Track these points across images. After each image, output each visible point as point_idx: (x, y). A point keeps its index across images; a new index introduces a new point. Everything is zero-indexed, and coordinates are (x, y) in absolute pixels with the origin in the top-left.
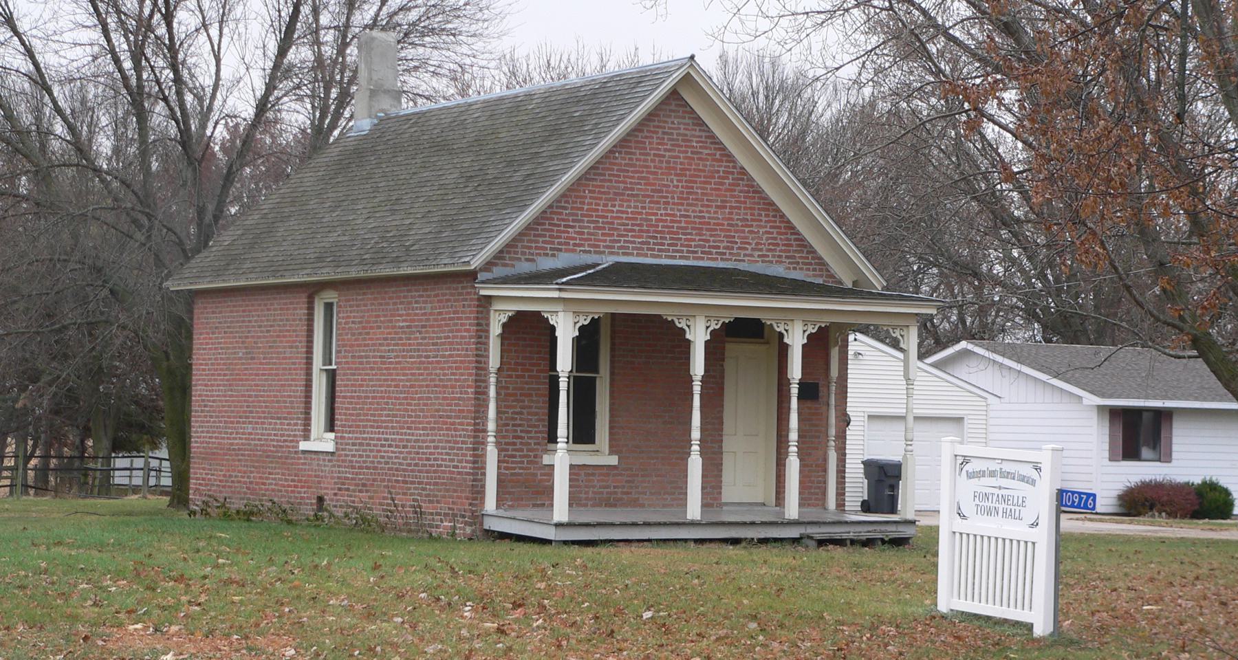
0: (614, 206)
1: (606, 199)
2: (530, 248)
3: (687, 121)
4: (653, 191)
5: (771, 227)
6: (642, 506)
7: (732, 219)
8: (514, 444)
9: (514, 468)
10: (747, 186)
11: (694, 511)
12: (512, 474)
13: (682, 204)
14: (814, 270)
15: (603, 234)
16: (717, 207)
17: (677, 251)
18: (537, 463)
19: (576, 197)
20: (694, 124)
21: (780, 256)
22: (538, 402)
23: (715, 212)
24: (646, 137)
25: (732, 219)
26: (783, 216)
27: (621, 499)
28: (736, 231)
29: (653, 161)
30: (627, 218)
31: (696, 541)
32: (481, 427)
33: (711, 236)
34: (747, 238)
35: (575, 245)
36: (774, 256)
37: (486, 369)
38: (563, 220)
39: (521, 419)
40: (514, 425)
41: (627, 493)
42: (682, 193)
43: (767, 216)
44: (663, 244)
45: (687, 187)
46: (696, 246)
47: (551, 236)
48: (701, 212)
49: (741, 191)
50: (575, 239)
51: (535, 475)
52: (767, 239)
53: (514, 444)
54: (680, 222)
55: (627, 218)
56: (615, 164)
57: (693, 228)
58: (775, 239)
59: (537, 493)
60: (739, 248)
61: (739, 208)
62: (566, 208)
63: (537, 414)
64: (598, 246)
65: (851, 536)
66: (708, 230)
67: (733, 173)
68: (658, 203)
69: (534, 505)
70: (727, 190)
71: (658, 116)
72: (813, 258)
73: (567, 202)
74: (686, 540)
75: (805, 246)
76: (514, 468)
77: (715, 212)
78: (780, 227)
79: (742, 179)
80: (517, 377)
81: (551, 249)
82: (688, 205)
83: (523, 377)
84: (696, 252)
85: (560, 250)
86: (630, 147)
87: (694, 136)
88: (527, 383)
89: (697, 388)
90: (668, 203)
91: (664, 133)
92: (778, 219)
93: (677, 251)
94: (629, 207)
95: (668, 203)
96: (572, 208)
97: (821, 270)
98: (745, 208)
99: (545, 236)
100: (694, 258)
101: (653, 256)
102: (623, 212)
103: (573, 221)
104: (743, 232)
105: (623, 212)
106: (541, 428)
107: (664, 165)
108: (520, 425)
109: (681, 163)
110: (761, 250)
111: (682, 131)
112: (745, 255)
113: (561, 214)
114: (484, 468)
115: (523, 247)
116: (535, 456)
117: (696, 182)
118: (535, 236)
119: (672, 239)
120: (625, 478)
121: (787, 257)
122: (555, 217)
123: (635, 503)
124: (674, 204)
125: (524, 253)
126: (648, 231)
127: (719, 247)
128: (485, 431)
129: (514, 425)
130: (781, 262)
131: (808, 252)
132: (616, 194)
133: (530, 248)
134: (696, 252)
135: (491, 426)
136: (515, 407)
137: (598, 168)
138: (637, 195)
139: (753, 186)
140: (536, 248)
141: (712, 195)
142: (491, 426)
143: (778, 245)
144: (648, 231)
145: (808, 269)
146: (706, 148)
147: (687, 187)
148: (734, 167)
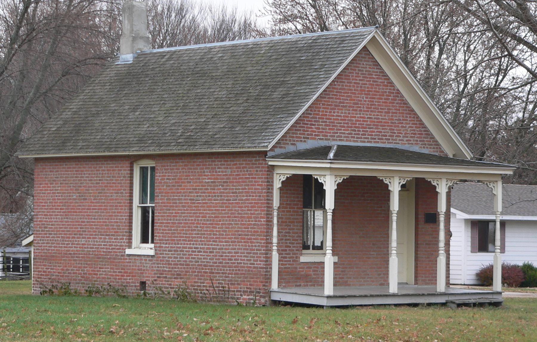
0: (334, 112)
1: (331, 109)
2: (293, 137)
3: (370, 63)
4: (354, 104)
5: (413, 124)
6: (349, 285)
7: (392, 119)
8: (286, 250)
9: (286, 265)
10: (400, 100)
12: (285, 268)
13: (368, 111)
14: (434, 148)
15: (329, 129)
16: (385, 112)
17: (366, 138)
18: (297, 261)
19: (316, 108)
20: (374, 65)
21: (417, 141)
22: (297, 226)
23: (385, 116)
24: (350, 73)
25: (392, 119)
26: (418, 117)
28: (395, 127)
29: (354, 86)
30: (341, 120)
31: (396, 305)
32: (269, 241)
33: (383, 129)
34: (400, 130)
35: (315, 135)
36: (414, 140)
37: (271, 207)
38: (310, 121)
39: (289, 236)
40: (286, 240)
42: (368, 104)
43: (410, 117)
44: (359, 134)
45: (371, 101)
46: (375, 135)
47: (304, 130)
48: (378, 115)
49: (397, 104)
50: (315, 132)
51: (296, 268)
52: (411, 130)
53: (286, 250)
54: (367, 121)
55: (341, 120)
56: (334, 88)
57: (374, 125)
58: (414, 130)
60: (397, 136)
61: (396, 113)
62: (311, 114)
63: (297, 233)
64: (327, 136)
65: (473, 301)
66: (381, 126)
67: (393, 93)
68: (356, 110)
69: (296, 286)
70: (390, 103)
72: (433, 141)
73: (311, 111)
74: (389, 305)
75: (429, 135)
76: (286, 265)
77: (385, 116)
78: (416, 124)
79: (398, 97)
80: (287, 211)
81: (304, 138)
82: (371, 111)
83: (290, 212)
84: (375, 139)
85: (308, 138)
86: (342, 79)
87: (374, 72)
88: (292, 215)
89: (394, 218)
90: (361, 111)
91: (359, 70)
92: (415, 119)
93: (366, 138)
94: (342, 113)
95: (361, 111)
96: (314, 114)
97: (437, 148)
98: (399, 113)
99: (300, 130)
100: (375, 142)
101: (354, 141)
102: (339, 116)
103: (315, 121)
104: (398, 126)
105: (339, 116)
106: (299, 242)
107: (359, 89)
108: (289, 240)
109: (368, 88)
110: (407, 137)
111: (368, 69)
112: (400, 140)
113: (308, 117)
114: (271, 264)
115: (290, 137)
116: (297, 257)
117: (374, 98)
118: (296, 130)
119: (363, 131)
120: (341, 269)
121: (420, 141)
122: (306, 119)
124: (364, 111)
125: (290, 141)
126: (351, 127)
127: (386, 136)
128: (272, 243)
129: (286, 240)
130: (418, 144)
131: (431, 138)
132: (335, 106)
133: (293, 137)
134: (375, 139)
135: (275, 240)
136: (286, 229)
138: (346, 106)
139: (403, 100)
140: (297, 137)
141: (383, 106)
142: (275, 240)
143: (415, 134)
144: (351, 127)
145: (431, 148)
146: (380, 79)
147: (371, 101)
148: (394, 90)
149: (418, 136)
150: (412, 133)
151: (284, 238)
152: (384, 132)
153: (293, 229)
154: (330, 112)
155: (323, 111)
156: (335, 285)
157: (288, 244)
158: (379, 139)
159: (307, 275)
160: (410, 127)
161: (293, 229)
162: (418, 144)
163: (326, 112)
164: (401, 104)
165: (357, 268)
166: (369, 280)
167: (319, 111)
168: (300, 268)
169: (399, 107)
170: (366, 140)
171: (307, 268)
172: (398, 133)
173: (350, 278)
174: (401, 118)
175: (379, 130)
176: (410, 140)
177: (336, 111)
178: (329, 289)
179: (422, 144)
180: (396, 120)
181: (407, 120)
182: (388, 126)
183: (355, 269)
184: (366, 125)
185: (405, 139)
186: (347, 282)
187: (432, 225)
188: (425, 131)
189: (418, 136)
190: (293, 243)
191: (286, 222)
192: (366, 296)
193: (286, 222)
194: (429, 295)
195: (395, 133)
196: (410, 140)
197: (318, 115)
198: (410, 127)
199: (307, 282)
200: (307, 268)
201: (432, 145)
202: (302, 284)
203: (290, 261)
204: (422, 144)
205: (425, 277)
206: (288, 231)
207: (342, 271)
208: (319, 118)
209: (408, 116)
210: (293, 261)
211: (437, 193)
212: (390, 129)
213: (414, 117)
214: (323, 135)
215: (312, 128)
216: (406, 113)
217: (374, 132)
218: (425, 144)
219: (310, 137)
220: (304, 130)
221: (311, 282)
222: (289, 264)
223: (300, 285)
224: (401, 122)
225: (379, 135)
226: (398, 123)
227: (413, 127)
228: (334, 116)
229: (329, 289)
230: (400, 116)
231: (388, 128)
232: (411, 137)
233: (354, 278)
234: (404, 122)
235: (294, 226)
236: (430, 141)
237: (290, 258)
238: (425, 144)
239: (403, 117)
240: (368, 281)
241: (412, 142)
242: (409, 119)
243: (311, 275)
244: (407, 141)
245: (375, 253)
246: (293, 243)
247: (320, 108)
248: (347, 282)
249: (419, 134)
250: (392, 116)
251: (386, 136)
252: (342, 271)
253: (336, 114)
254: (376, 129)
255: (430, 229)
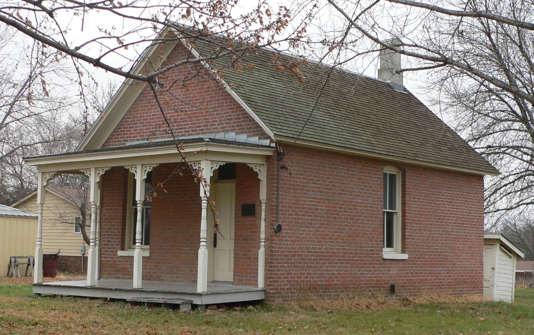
0: (151, 112)
1: (148, 110)
5: (229, 109)
6: (162, 280)
7: (207, 108)
8: (107, 245)
12: (107, 261)
14: (254, 131)
16: (200, 103)
19: (135, 111)
21: (233, 126)
22: (117, 222)
25: (207, 108)
27: (152, 276)
33: (197, 120)
34: (215, 118)
36: (229, 127)
38: (129, 125)
39: (111, 232)
41: (156, 273)
43: (226, 102)
46: (189, 128)
49: (212, 91)
50: (133, 134)
51: (116, 261)
52: (226, 117)
55: (157, 118)
58: (230, 116)
59: (117, 271)
62: (130, 118)
63: (117, 229)
64: (143, 136)
66: (195, 117)
69: (116, 278)
70: (205, 92)
71: (172, 58)
73: (131, 115)
76: (107, 258)
78: (233, 108)
84: (189, 131)
88: (113, 213)
92: (232, 103)
98: (215, 100)
102: (154, 115)
104: (213, 115)
105: (154, 115)
106: (119, 237)
110: (222, 124)
112: (214, 129)
113: (128, 121)
119: (177, 125)
120: (154, 264)
121: (237, 126)
123: (159, 279)
130: (234, 129)
134: (189, 131)
136: (108, 225)
137: (144, 94)
140: (118, 141)
141: (197, 96)
143: (232, 119)
145: (250, 132)
147: (185, 94)
149: (235, 121)
150: (227, 120)
151: (107, 234)
152: (198, 123)
153: (114, 225)
154: (147, 113)
155: (141, 114)
156: (143, 279)
157: (110, 239)
158: (192, 131)
159: (125, 268)
160: (226, 113)
161: (114, 225)
162: (234, 129)
163: (144, 113)
164: (216, 90)
165: (170, 263)
166: (181, 276)
167: (137, 114)
168: (119, 261)
169: (215, 94)
170: (180, 134)
171: (125, 261)
172: (213, 122)
173: (163, 273)
174: (216, 105)
175: (193, 122)
176: (226, 127)
177: (152, 111)
178: (137, 282)
179: (239, 129)
180: (211, 108)
181: (223, 106)
182: (202, 116)
183: (168, 265)
184: (181, 119)
185: (220, 127)
186: (159, 277)
187: (250, 218)
188: (242, 114)
189: (235, 121)
190: (114, 239)
191: (108, 219)
193: (108, 219)
194: (116, 290)
195: (209, 122)
196: (226, 127)
197: (136, 117)
198: (226, 113)
199: (124, 275)
200: (125, 261)
201: (251, 128)
202: (121, 276)
203: (111, 255)
204: (239, 129)
205: (242, 276)
206: (110, 227)
207: (156, 266)
208: (137, 120)
209: (224, 101)
210: (114, 255)
211: (259, 181)
212: (204, 119)
213: (231, 102)
214: (140, 136)
215: (131, 131)
216: (222, 99)
217: (187, 124)
218: (244, 129)
219: (128, 139)
220: (124, 134)
221: (128, 275)
222: (110, 258)
223: (119, 278)
224: (217, 109)
225: (193, 127)
226: (213, 111)
227: (229, 113)
228: (150, 116)
229: (137, 282)
230: (215, 104)
231: (203, 118)
232: (227, 123)
233: (167, 273)
234: (220, 109)
235: (115, 222)
236: (249, 125)
237: (110, 252)
238: (244, 129)
239: (218, 103)
240: (181, 277)
241: (228, 129)
242: (224, 105)
243: (127, 268)
244: (221, 128)
245: (188, 249)
246: (114, 239)
247: (138, 110)
248: (159, 277)
249: (235, 119)
250: (207, 105)
251: (200, 126)
252: (156, 266)
253: (152, 113)
254: (190, 121)
255: (248, 223)
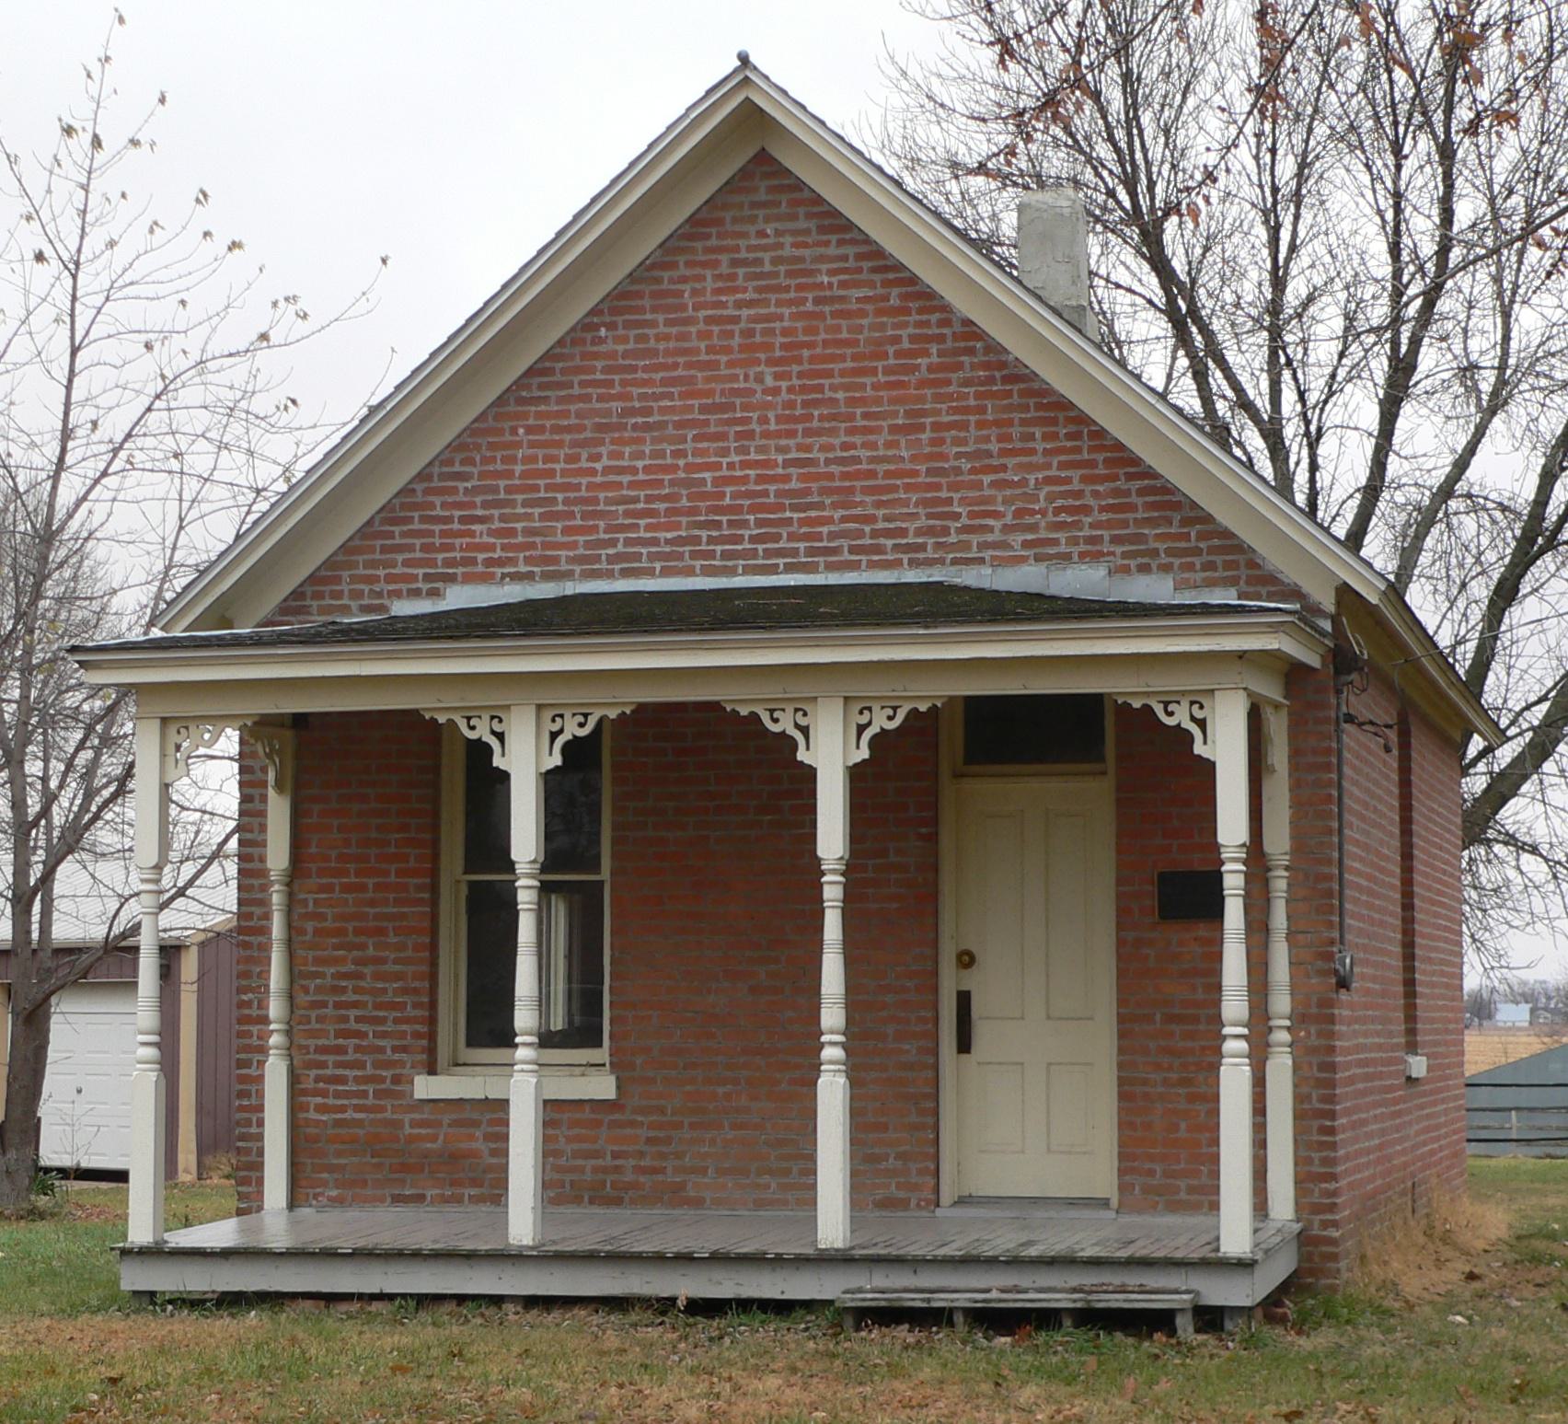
0: (597, 458)
1: (574, 444)
2: (372, 580)
3: (802, 224)
4: (703, 409)
6: (698, 1203)
7: (942, 457)
8: (340, 1050)
9: (342, 1109)
10: (986, 366)
11: (832, 1222)
12: (338, 1123)
13: (791, 434)
14: (1209, 566)
15: (567, 531)
16: (894, 429)
17: (780, 553)
18: (400, 1095)
20: (822, 230)
22: (401, 947)
23: (889, 445)
24: (684, 280)
25: (942, 457)
26: (1101, 433)
27: (635, 1186)
28: (954, 487)
29: (702, 335)
30: (632, 485)
31: (531, 1302)
32: (254, 1012)
33: (879, 504)
35: (490, 562)
37: (263, 873)
39: (356, 990)
40: (337, 1005)
41: (655, 1171)
42: (790, 405)
44: (737, 539)
45: (804, 389)
47: (425, 548)
48: (845, 446)
50: (492, 548)
53: (340, 1050)
54: (787, 478)
55: (632, 485)
56: (596, 356)
57: (824, 491)
58: (1078, 494)
59: (404, 1168)
60: (967, 529)
61: (963, 426)
63: (398, 977)
64: (556, 560)
65: (962, 1300)
66: (868, 491)
67: (940, 339)
68: (722, 437)
69: (398, 1199)
71: (718, 222)
72: (1202, 536)
73: (469, 461)
74: (497, 1300)
75: (1177, 506)
76: (342, 1109)
77: (889, 445)
78: (1092, 464)
79: (971, 351)
80: (347, 888)
81: (427, 578)
82: (808, 433)
83: (363, 888)
85: (451, 579)
86: (642, 310)
87: (821, 259)
88: (372, 903)
90: (749, 435)
91: (735, 263)
92: (1086, 443)
93: (780, 553)
94: (639, 455)
95: (749, 435)
96: (482, 475)
97: (1228, 565)
98: (981, 425)
99: (411, 548)
100: (831, 567)
101: (709, 572)
103: (485, 505)
104: (978, 485)
106: (410, 1012)
107: (736, 341)
108: (355, 1005)
109: (785, 332)
110: (1033, 528)
111: (788, 251)
112: (983, 546)
114: (260, 1108)
115: (354, 579)
116: (397, 1080)
117: (829, 374)
118: (384, 550)
120: (643, 1133)
121: (1116, 540)
122: (437, 500)
123: (675, 1196)
124: (766, 435)
125: (357, 595)
126: (692, 511)
127: (903, 532)
128: (265, 1020)
129: (337, 1005)
130: (1101, 554)
131: (1186, 522)
132: (600, 428)
133: (372, 580)
135: (275, 1008)
136: (342, 960)
137: (550, 371)
138: (661, 425)
139: (1003, 365)
140: (390, 579)
142: (275, 1008)
143: (1086, 510)
144: (692, 511)
145: (1190, 567)
146: (857, 284)
147: (804, 389)
148: (945, 323)
150: (1057, 511)
151: (331, 999)
155: (527, 460)
157: (353, 1025)
160: (1049, 481)
162: (1101, 554)
164: (991, 381)
165: (734, 1126)
167: (513, 460)
168: (414, 1124)
170: (781, 561)
174: (994, 447)
180: (959, 455)
186: (681, 1187)
192: (685, 1259)
195: (957, 516)
198: (1049, 481)
199: (454, 1183)
201: (1197, 552)
202: (429, 1194)
215: (472, 534)
219: (460, 570)
221: (475, 1183)
222: (358, 1108)
223: (420, 1198)
233: (721, 1172)
243: (473, 1154)
247: (518, 445)
248: (681, 1187)
249: (1102, 509)
253: (605, 461)
254: (835, 506)
